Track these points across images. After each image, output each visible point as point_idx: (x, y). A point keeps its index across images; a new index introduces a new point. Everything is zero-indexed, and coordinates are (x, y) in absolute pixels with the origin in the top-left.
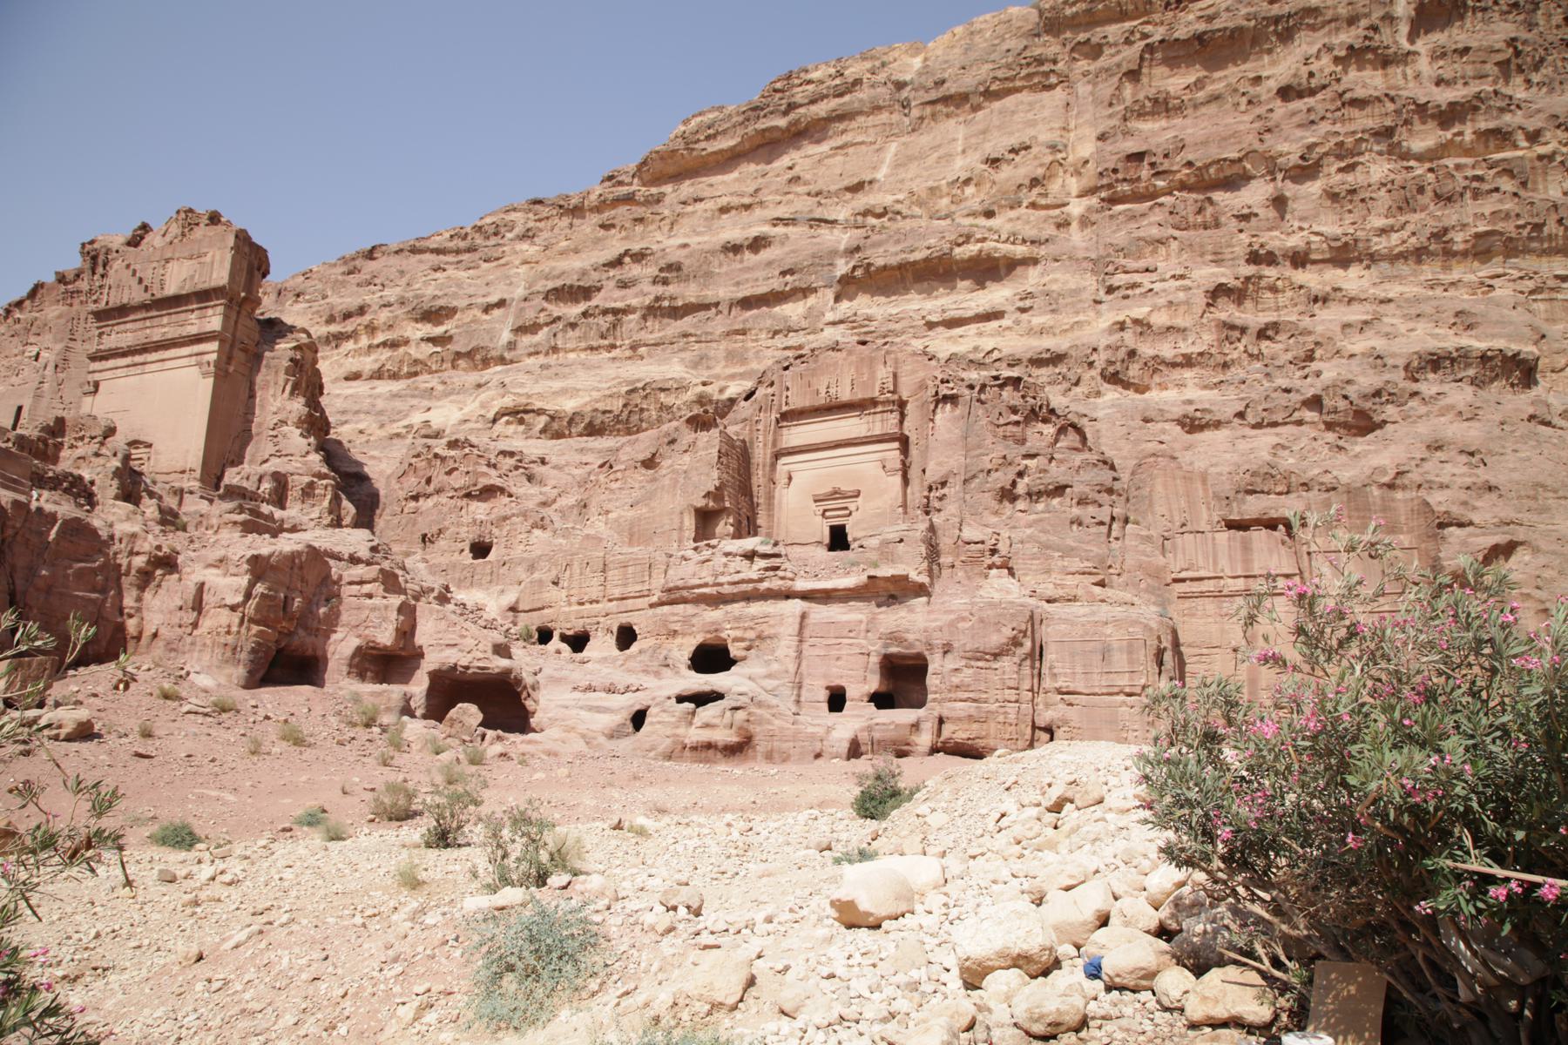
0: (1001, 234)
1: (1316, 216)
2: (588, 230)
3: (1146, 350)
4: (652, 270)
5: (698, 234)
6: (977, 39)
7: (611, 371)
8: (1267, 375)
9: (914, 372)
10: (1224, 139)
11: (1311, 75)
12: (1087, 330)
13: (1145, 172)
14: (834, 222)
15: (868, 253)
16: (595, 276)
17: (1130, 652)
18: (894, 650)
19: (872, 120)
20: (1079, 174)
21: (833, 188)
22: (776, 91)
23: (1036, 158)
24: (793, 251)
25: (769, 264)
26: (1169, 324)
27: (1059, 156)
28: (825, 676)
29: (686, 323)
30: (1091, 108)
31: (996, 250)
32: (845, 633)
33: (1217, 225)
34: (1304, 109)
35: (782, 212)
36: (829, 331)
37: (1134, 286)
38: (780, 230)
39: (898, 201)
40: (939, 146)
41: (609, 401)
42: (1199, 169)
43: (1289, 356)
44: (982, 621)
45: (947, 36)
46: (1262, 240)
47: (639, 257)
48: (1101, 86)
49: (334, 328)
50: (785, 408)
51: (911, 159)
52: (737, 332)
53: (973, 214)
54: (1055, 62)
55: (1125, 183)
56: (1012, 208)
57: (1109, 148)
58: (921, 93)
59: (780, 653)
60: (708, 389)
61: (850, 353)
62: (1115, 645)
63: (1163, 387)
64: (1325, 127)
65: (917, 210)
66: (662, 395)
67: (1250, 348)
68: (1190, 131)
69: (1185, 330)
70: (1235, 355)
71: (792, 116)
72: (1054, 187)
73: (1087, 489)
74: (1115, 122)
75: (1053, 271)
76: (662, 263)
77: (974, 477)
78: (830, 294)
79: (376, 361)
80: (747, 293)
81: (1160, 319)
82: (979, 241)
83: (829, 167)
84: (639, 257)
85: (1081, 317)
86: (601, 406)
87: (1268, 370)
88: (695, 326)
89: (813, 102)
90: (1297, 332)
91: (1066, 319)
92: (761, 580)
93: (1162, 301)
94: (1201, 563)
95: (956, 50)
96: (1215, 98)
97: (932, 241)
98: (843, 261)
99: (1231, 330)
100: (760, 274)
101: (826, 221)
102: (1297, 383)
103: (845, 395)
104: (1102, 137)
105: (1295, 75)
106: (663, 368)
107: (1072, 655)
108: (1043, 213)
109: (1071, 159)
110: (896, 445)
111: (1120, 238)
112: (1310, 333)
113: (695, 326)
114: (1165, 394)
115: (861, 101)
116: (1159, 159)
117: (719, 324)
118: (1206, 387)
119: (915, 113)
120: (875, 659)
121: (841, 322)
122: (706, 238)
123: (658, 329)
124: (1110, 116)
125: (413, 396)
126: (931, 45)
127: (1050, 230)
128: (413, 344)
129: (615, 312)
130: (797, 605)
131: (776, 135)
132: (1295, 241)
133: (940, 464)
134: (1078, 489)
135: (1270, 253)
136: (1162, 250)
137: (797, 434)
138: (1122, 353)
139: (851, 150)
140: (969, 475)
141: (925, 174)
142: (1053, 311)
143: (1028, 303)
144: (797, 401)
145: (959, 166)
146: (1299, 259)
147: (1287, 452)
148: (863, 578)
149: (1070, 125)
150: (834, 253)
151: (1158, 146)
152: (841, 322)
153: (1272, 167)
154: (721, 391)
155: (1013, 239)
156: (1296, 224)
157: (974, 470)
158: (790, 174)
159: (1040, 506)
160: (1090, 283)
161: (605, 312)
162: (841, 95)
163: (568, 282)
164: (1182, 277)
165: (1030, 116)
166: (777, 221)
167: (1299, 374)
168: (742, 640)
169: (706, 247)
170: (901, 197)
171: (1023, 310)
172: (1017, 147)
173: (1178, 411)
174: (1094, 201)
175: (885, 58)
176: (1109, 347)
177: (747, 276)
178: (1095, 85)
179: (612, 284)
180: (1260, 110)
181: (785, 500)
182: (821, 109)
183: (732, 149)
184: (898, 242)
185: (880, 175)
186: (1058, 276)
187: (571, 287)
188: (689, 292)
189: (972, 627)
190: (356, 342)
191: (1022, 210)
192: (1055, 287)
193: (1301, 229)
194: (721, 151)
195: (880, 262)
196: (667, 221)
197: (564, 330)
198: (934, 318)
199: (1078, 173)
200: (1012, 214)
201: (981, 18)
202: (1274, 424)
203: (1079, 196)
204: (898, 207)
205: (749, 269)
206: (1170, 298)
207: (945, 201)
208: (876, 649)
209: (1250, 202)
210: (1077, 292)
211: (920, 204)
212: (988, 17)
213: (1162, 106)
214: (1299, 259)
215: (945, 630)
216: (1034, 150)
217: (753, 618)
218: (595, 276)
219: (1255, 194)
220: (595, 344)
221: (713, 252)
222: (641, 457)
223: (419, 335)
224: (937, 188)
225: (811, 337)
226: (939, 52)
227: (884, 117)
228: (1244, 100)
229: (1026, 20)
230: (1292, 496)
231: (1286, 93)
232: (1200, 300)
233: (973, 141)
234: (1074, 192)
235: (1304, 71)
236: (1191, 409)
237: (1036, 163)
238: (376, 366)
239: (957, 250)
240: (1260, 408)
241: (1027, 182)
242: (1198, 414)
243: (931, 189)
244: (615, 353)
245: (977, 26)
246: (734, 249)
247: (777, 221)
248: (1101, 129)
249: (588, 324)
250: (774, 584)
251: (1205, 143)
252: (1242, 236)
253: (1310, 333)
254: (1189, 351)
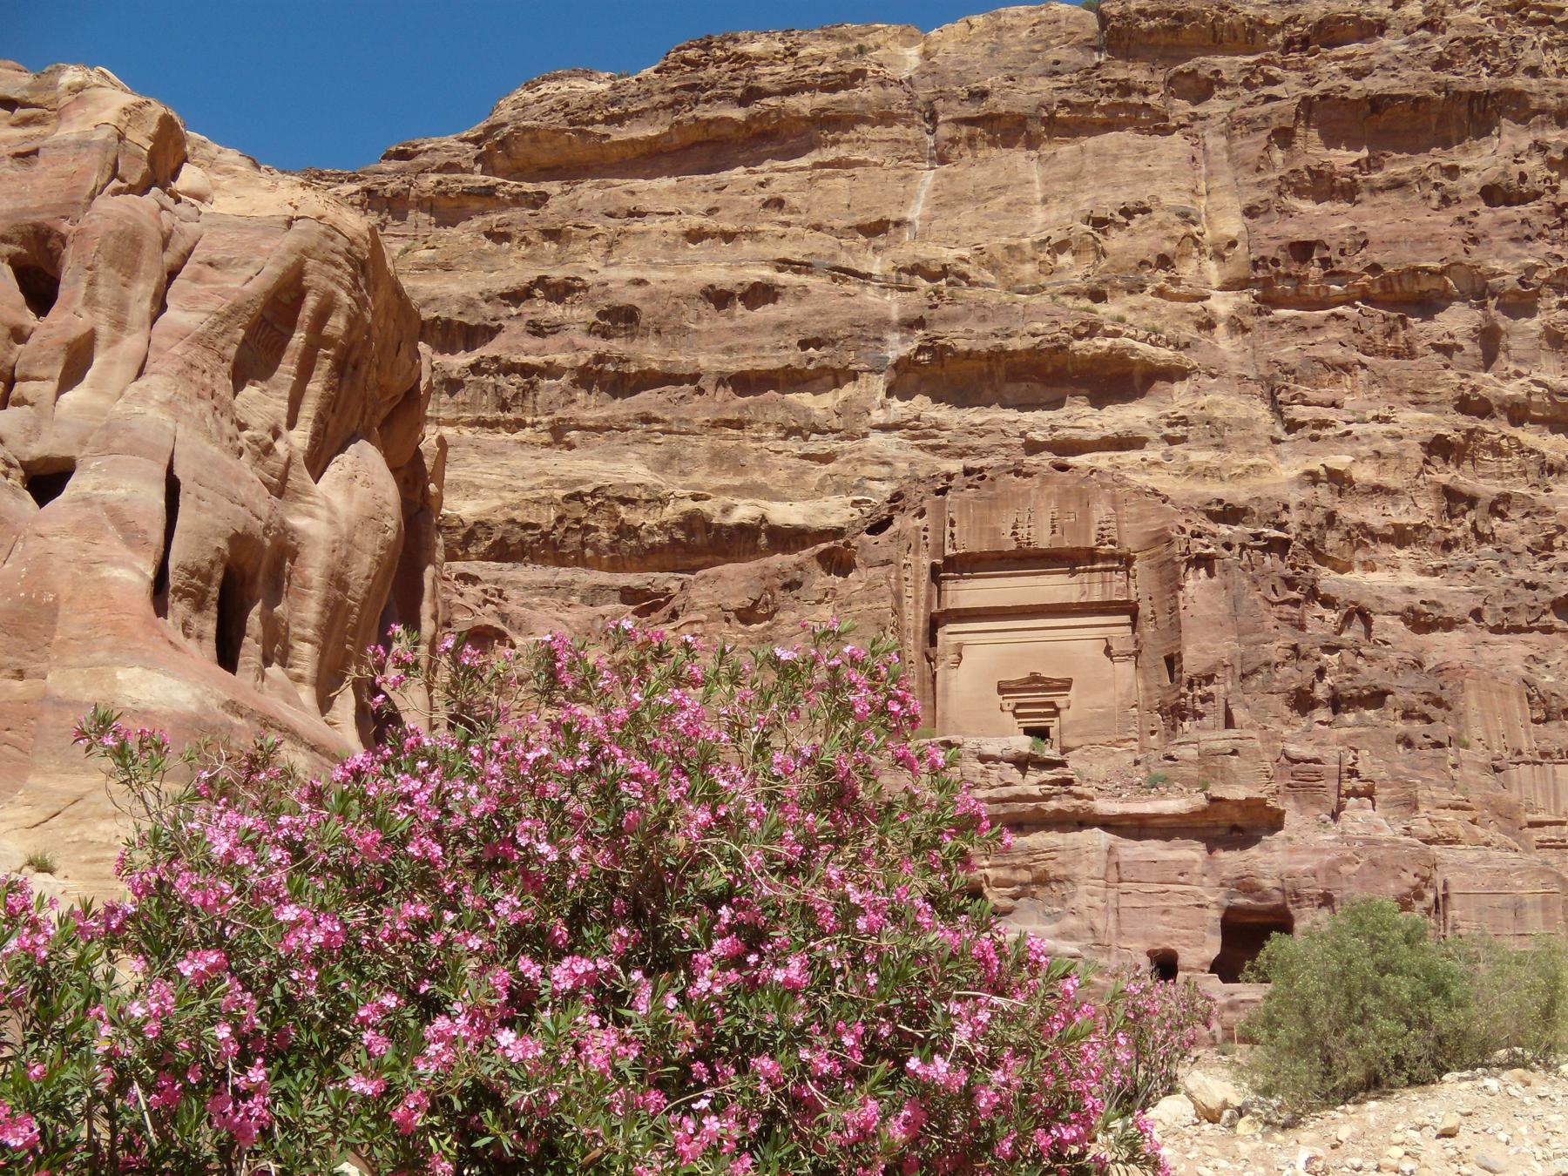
0: (1132, 324)
1: (1535, 360)
2: (467, 238)
3: (1350, 513)
5: (656, 266)
6: (1007, 38)
7: (524, 461)
8: (1504, 562)
9: (1141, 517)
10: (1419, 241)
11: (1523, 177)
12: (1267, 479)
13: (1314, 271)
14: (868, 276)
15: (939, 329)
16: (488, 310)
17: (1545, 910)
18: (1241, 901)
19: (881, 132)
20: (1223, 258)
21: (839, 223)
22: (686, 61)
23: (1161, 226)
24: (818, 312)
25: (781, 326)
26: (1375, 481)
27: (1194, 229)
28: (1145, 936)
29: (648, 400)
30: (1228, 169)
31: (1133, 350)
32: (1173, 876)
33: (1412, 354)
34: (1518, 218)
35: (786, 250)
36: (876, 440)
37: (1324, 424)
38: (785, 278)
39: (962, 259)
40: (1006, 187)
41: (533, 509)
42: (1389, 276)
43: (1526, 540)
44: (1373, 863)
45: (960, 26)
46: (1473, 383)
47: (560, 292)
48: (1239, 141)
50: (949, 552)
51: (961, 199)
52: (729, 423)
53: (1075, 293)
54: (1145, 93)
55: (1283, 279)
56: (1131, 292)
57: (1265, 230)
58: (954, 104)
59: (1081, 901)
60: (705, 506)
61: (1046, 480)
62: (1528, 900)
63: (1369, 566)
64: (1542, 247)
65: (988, 276)
66: (622, 509)
67: (1480, 524)
68: (1372, 223)
69: (1396, 492)
70: (1459, 533)
71: (755, 108)
72: (1187, 270)
73: (1413, 698)
74: (1264, 194)
75: (1211, 390)
76: (603, 304)
77: (1255, 671)
78: (879, 384)
80: (746, 366)
81: (1365, 474)
82: (1107, 335)
83: (827, 192)
84: (560, 292)
85: (1256, 460)
86: (519, 515)
87: (1504, 556)
88: (660, 406)
89: (788, 91)
90: (1534, 511)
91: (1238, 460)
92: (1046, 797)
93: (1365, 449)
94: (1540, 804)
95: (978, 49)
96: (1397, 185)
97: (1040, 326)
98: (897, 336)
99: (1455, 500)
100: (767, 340)
101: (856, 274)
102: (1544, 578)
103: (1043, 540)
104: (1250, 212)
105: (1504, 174)
106: (620, 466)
107: (1480, 911)
108: (1178, 305)
109: (1208, 235)
110: (1126, 619)
111: (1289, 353)
112: (1549, 513)
113: (660, 406)
114: (1372, 576)
115: (864, 101)
116: (1335, 256)
117: (701, 409)
118: (1423, 572)
119: (944, 131)
120: (1214, 915)
121: (897, 427)
122: (670, 275)
123: (591, 407)
124: (1259, 185)
126: (934, 33)
127: (1188, 332)
129: (526, 370)
130: (1098, 838)
131: (727, 130)
132: (1512, 389)
133: (1202, 650)
134: (1402, 697)
135: (1484, 401)
136: (1347, 380)
137: (969, 592)
138: (1318, 516)
139: (858, 171)
140: (1249, 668)
141: (989, 223)
142: (1217, 446)
143: (1179, 431)
144: (968, 541)
145: (1041, 221)
146: (1518, 413)
147: (1541, 667)
148: (1200, 801)
149: (1194, 184)
150: (884, 323)
151: (1332, 236)
152: (897, 427)
153: (1479, 290)
154: (726, 511)
155: (1153, 336)
156: (1512, 367)
157: (1255, 662)
158: (766, 194)
159: (1350, 717)
160: (1262, 411)
161: (510, 369)
162: (833, 89)
163: (444, 315)
164: (1386, 420)
165: (1142, 165)
166: (784, 264)
167: (1542, 565)
168: (1011, 884)
169: (677, 289)
170: (966, 253)
171: (1172, 441)
172: (1131, 206)
173: (1401, 602)
174: (1245, 298)
175: (862, 40)
176: (1302, 505)
177: (744, 340)
178: (1230, 138)
180: (1463, 210)
181: (952, 685)
182: (803, 103)
183: (650, 141)
184: (983, 319)
185: (915, 212)
186: (1220, 398)
187: (448, 322)
188: (650, 353)
189: (1361, 872)
191: (1146, 298)
192: (1218, 413)
193: (1519, 375)
194: (632, 141)
195: (962, 345)
196: (602, 241)
198: (1038, 436)
199: (1219, 256)
200: (1133, 300)
201: (1012, 10)
202: (1518, 630)
203: (1221, 289)
204: (964, 267)
205: (746, 331)
206: (1376, 446)
207: (1029, 269)
208: (1215, 899)
209: (1452, 330)
210: (1248, 423)
211: (994, 267)
212: (1022, 9)
213: (1323, 186)
214: (1518, 413)
215: (1321, 876)
216: (1158, 216)
217: (1030, 852)
218: (488, 310)
219: (1457, 321)
220: (488, 415)
221: (688, 298)
222: (735, 603)
224: (1018, 248)
225: (847, 444)
226: (950, 48)
227: (898, 130)
228: (1436, 194)
229: (1083, 25)
230: (1553, 725)
231: (1493, 194)
232: (1416, 454)
233: (1058, 187)
234: (1215, 284)
235: (1515, 170)
236: (1416, 599)
237: (1163, 234)
239: (1077, 344)
240: (1500, 606)
241: (1152, 259)
242: (1424, 608)
243: (1008, 248)
245: (1006, 20)
246: (719, 298)
247: (784, 264)
248: (1247, 200)
249: (480, 385)
250: (1066, 804)
251: (1394, 242)
252: (1450, 374)
253: (1549, 513)
254: (1404, 520)
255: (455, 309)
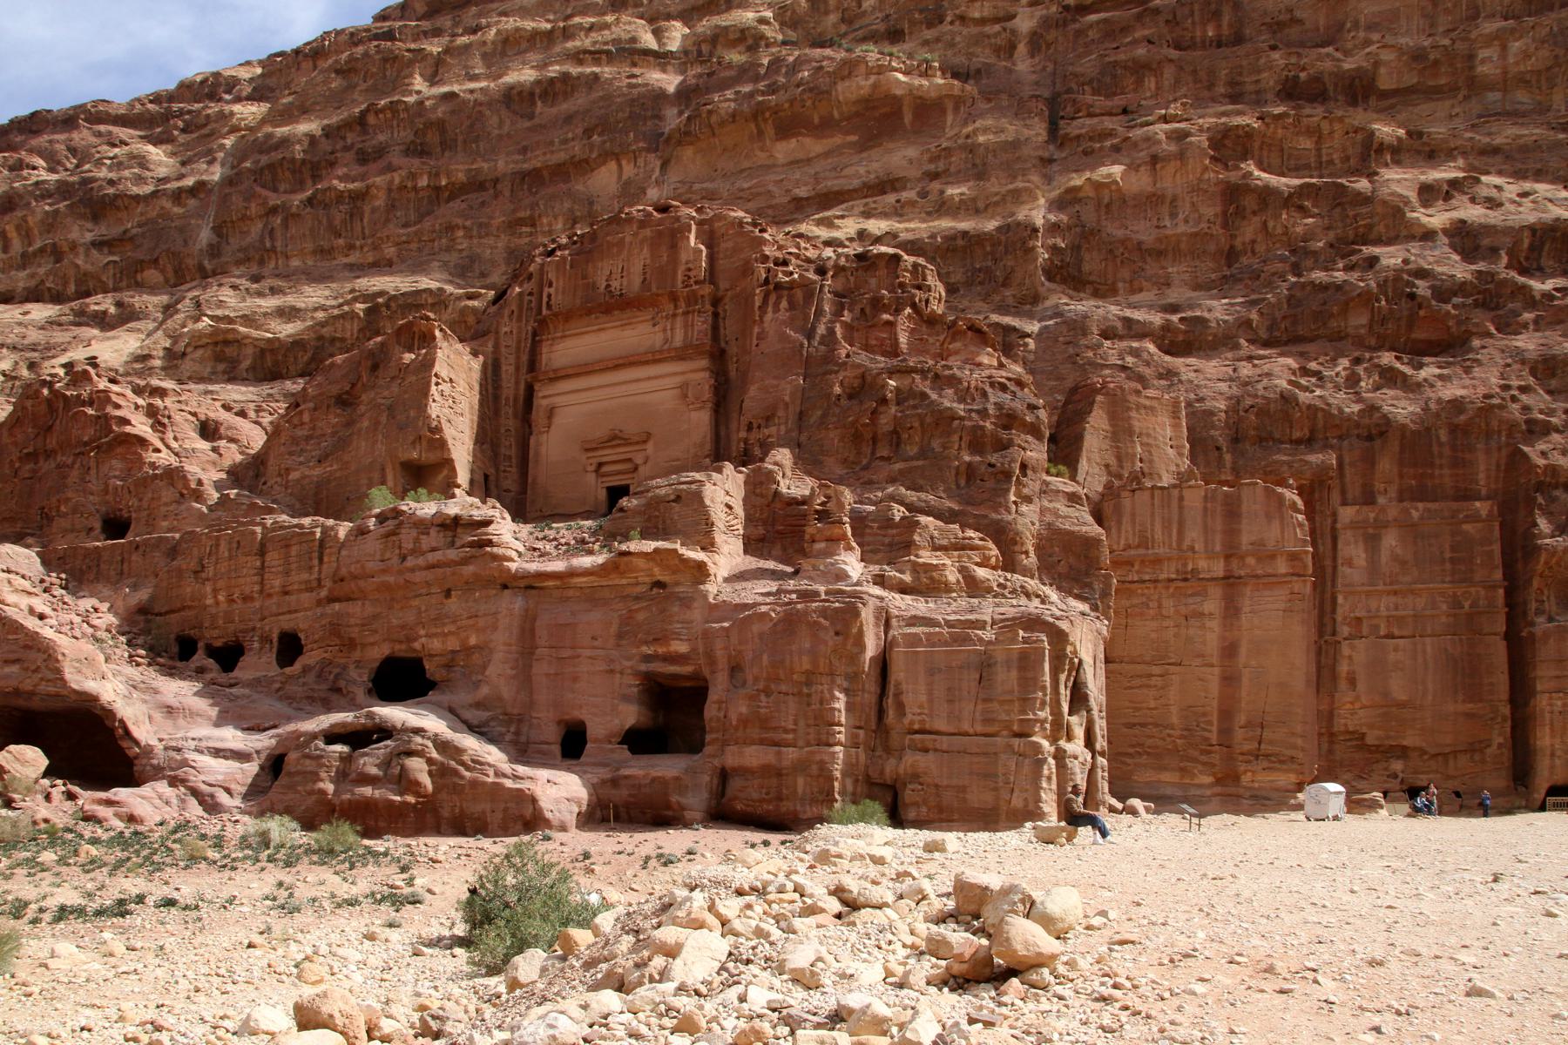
4: (406, 135)
25: (569, 119)
79: (32, 276)
128: (81, 250)
179: (350, 155)
197: (285, 225)
220: (325, 244)
223: (89, 237)
238: (33, 283)
244: (354, 258)
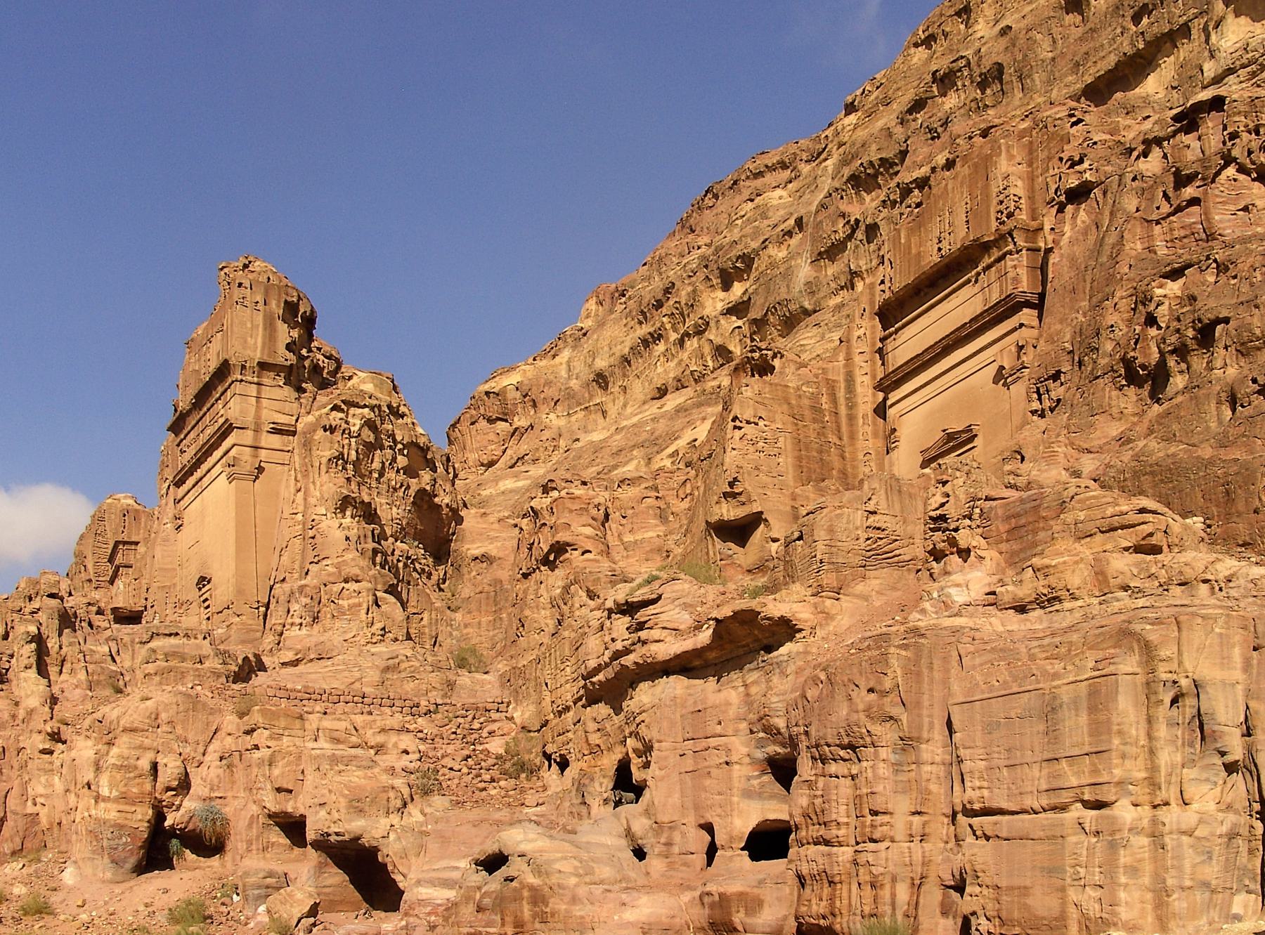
49: (645, 330)
62: (1065, 694)
92: (627, 651)
125: (699, 405)
128: (712, 324)
163: (865, 160)
190: (667, 340)
223: (720, 306)
255: (874, 147)
